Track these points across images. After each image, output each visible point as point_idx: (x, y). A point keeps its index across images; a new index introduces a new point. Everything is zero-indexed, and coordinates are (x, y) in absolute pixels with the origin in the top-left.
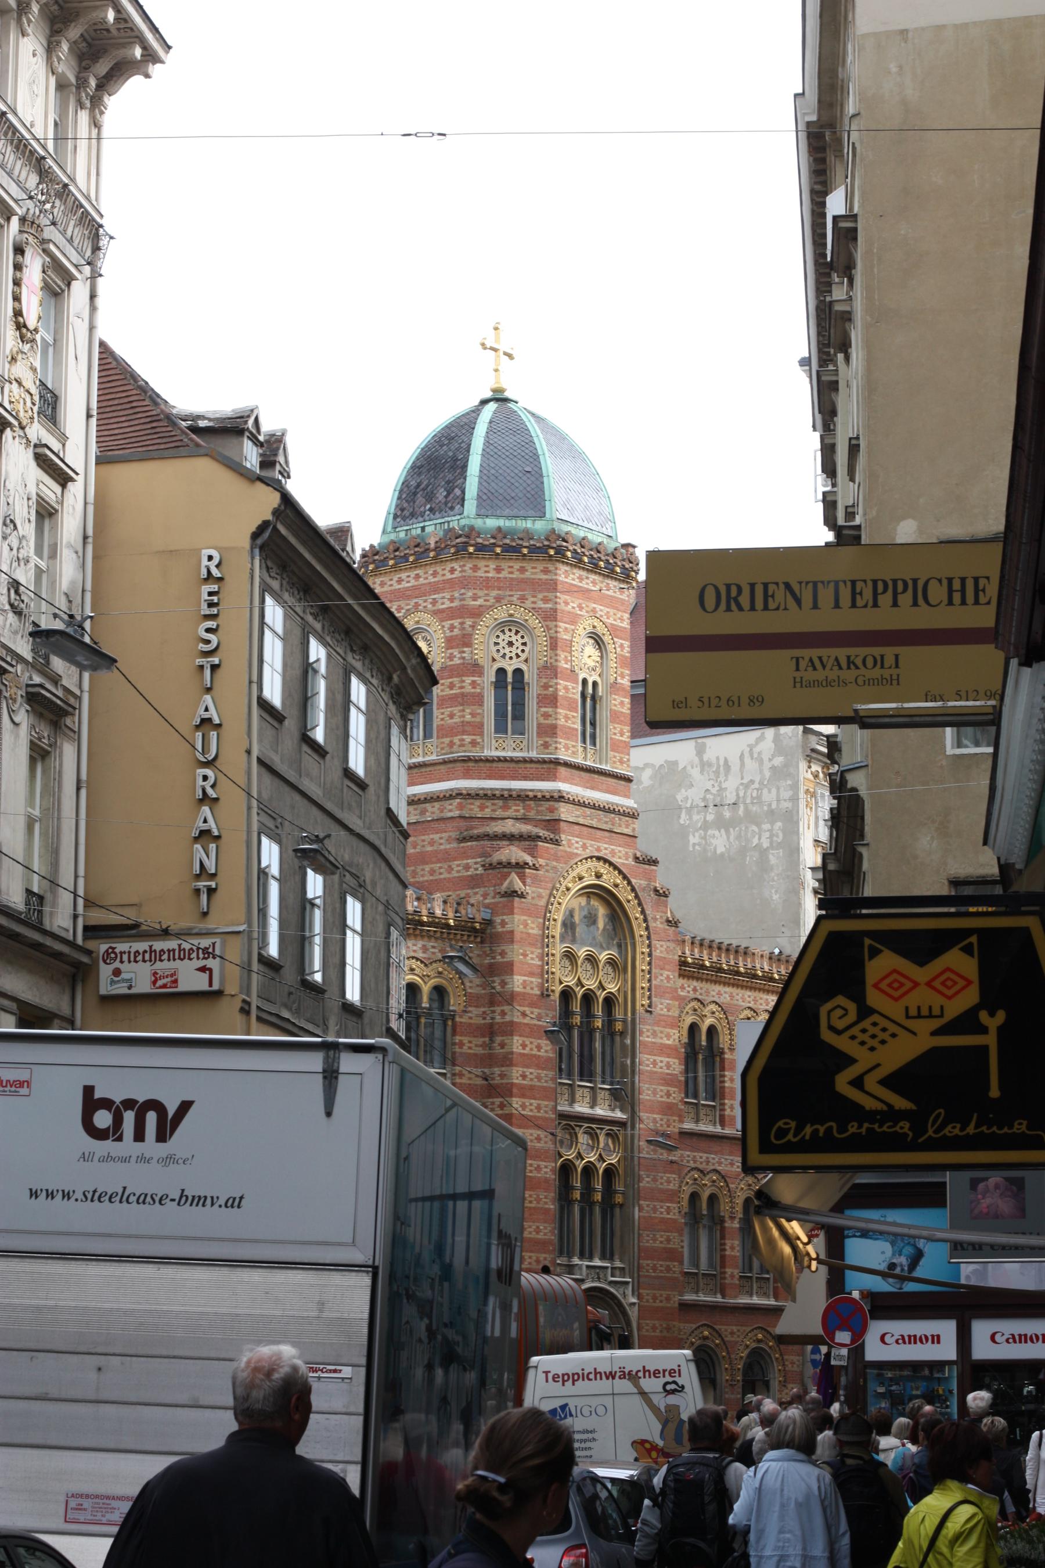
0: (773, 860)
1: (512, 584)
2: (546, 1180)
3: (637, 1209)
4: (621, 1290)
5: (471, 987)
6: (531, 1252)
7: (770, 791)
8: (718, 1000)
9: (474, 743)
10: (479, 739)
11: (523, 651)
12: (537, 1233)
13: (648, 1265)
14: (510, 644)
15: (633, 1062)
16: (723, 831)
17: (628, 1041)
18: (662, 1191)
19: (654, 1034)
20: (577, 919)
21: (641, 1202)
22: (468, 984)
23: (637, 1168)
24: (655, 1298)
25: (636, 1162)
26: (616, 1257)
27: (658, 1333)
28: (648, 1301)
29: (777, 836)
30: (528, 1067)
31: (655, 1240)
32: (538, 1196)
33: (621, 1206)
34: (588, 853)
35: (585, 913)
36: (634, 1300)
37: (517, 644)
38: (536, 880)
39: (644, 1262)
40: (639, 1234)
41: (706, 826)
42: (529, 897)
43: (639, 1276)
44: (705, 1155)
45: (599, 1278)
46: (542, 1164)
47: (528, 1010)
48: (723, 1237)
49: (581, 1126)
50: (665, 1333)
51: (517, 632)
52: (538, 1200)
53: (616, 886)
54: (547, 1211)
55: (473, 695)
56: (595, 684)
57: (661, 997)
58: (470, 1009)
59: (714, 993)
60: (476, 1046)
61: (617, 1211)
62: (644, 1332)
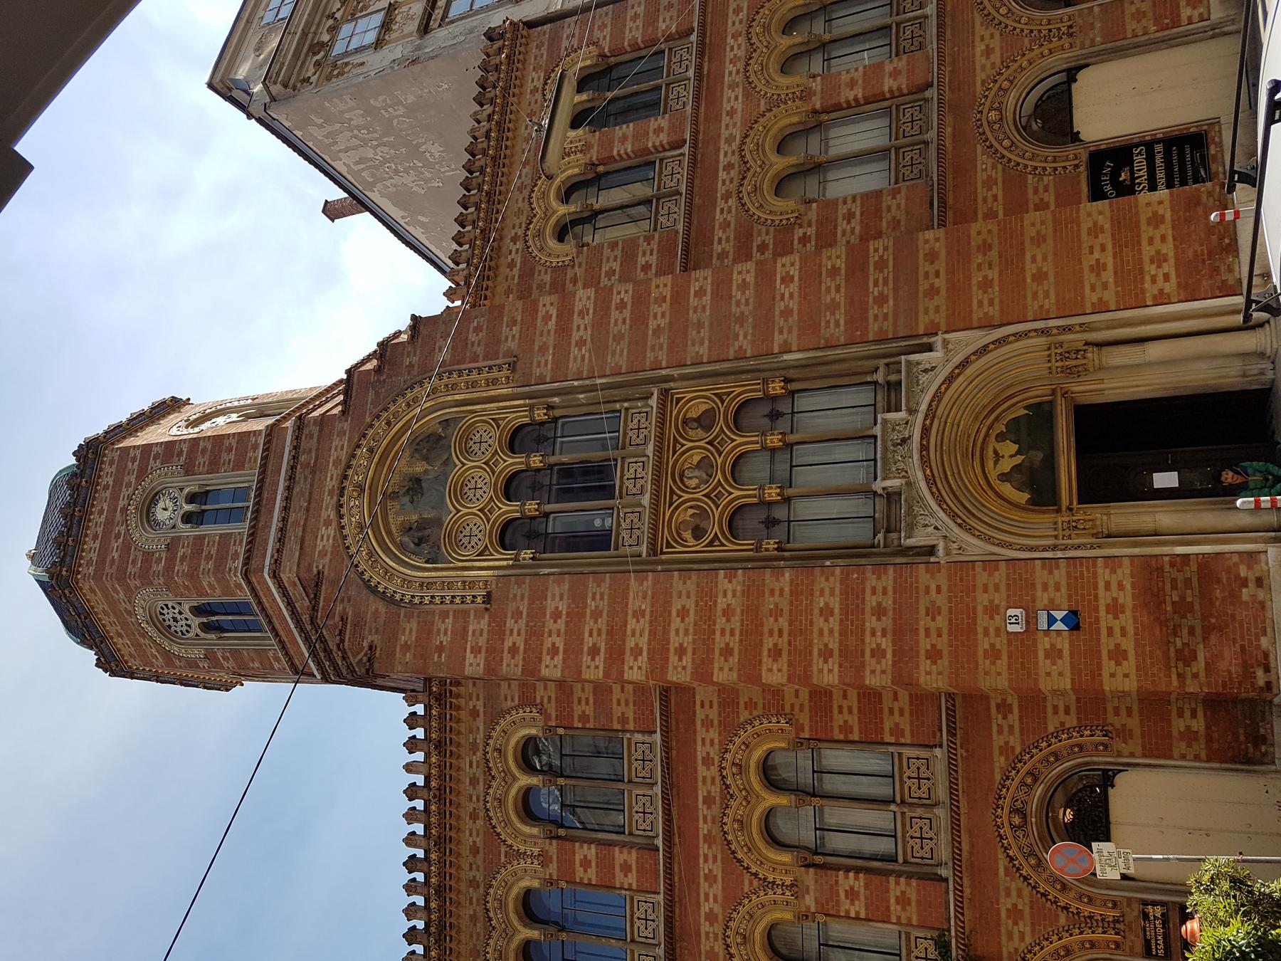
0: (411, 99)
1: (124, 624)
2: (746, 593)
3: (786, 357)
4: (924, 378)
5: (513, 700)
6: (863, 631)
7: (351, 119)
8: (529, 189)
9: (277, 659)
10: (271, 654)
11: (173, 608)
13: (876, 316)
14: (175, 620)
16: (423, 149)
17: (556, 399)
19: (543, 349)
20: (415, 517)
22: (509, 704)
23: (726, 365)
24: (933, 292)
25: (717, 367)
26: (869, 379)
27: (993, 274)
28: (937, 310)
29: (385, 100)
31: (834, 306)
33: (787, 380)
34: (333, 515)
35: (406, 499)
36: (938, 340)
37: (171, 615)
38: (359, 626)
39: (873, 327)
41: (428, 165)
42: (376, 638)
43: (895, 339)
44: (722, 175)
45: (904, 441)
46: (721, 603)
47: (508, 643)
48: (838, 107)
50: (994, 254)
51: (161, 614)
52: (777, 612)
53: (371, 450)
54: (795, 593)
55: (236, 660)
56: (191, 499)
57: (499, 341)
58: (538, 701)
59: (520, 204)
60: (583, 690)
62: (994, 311)
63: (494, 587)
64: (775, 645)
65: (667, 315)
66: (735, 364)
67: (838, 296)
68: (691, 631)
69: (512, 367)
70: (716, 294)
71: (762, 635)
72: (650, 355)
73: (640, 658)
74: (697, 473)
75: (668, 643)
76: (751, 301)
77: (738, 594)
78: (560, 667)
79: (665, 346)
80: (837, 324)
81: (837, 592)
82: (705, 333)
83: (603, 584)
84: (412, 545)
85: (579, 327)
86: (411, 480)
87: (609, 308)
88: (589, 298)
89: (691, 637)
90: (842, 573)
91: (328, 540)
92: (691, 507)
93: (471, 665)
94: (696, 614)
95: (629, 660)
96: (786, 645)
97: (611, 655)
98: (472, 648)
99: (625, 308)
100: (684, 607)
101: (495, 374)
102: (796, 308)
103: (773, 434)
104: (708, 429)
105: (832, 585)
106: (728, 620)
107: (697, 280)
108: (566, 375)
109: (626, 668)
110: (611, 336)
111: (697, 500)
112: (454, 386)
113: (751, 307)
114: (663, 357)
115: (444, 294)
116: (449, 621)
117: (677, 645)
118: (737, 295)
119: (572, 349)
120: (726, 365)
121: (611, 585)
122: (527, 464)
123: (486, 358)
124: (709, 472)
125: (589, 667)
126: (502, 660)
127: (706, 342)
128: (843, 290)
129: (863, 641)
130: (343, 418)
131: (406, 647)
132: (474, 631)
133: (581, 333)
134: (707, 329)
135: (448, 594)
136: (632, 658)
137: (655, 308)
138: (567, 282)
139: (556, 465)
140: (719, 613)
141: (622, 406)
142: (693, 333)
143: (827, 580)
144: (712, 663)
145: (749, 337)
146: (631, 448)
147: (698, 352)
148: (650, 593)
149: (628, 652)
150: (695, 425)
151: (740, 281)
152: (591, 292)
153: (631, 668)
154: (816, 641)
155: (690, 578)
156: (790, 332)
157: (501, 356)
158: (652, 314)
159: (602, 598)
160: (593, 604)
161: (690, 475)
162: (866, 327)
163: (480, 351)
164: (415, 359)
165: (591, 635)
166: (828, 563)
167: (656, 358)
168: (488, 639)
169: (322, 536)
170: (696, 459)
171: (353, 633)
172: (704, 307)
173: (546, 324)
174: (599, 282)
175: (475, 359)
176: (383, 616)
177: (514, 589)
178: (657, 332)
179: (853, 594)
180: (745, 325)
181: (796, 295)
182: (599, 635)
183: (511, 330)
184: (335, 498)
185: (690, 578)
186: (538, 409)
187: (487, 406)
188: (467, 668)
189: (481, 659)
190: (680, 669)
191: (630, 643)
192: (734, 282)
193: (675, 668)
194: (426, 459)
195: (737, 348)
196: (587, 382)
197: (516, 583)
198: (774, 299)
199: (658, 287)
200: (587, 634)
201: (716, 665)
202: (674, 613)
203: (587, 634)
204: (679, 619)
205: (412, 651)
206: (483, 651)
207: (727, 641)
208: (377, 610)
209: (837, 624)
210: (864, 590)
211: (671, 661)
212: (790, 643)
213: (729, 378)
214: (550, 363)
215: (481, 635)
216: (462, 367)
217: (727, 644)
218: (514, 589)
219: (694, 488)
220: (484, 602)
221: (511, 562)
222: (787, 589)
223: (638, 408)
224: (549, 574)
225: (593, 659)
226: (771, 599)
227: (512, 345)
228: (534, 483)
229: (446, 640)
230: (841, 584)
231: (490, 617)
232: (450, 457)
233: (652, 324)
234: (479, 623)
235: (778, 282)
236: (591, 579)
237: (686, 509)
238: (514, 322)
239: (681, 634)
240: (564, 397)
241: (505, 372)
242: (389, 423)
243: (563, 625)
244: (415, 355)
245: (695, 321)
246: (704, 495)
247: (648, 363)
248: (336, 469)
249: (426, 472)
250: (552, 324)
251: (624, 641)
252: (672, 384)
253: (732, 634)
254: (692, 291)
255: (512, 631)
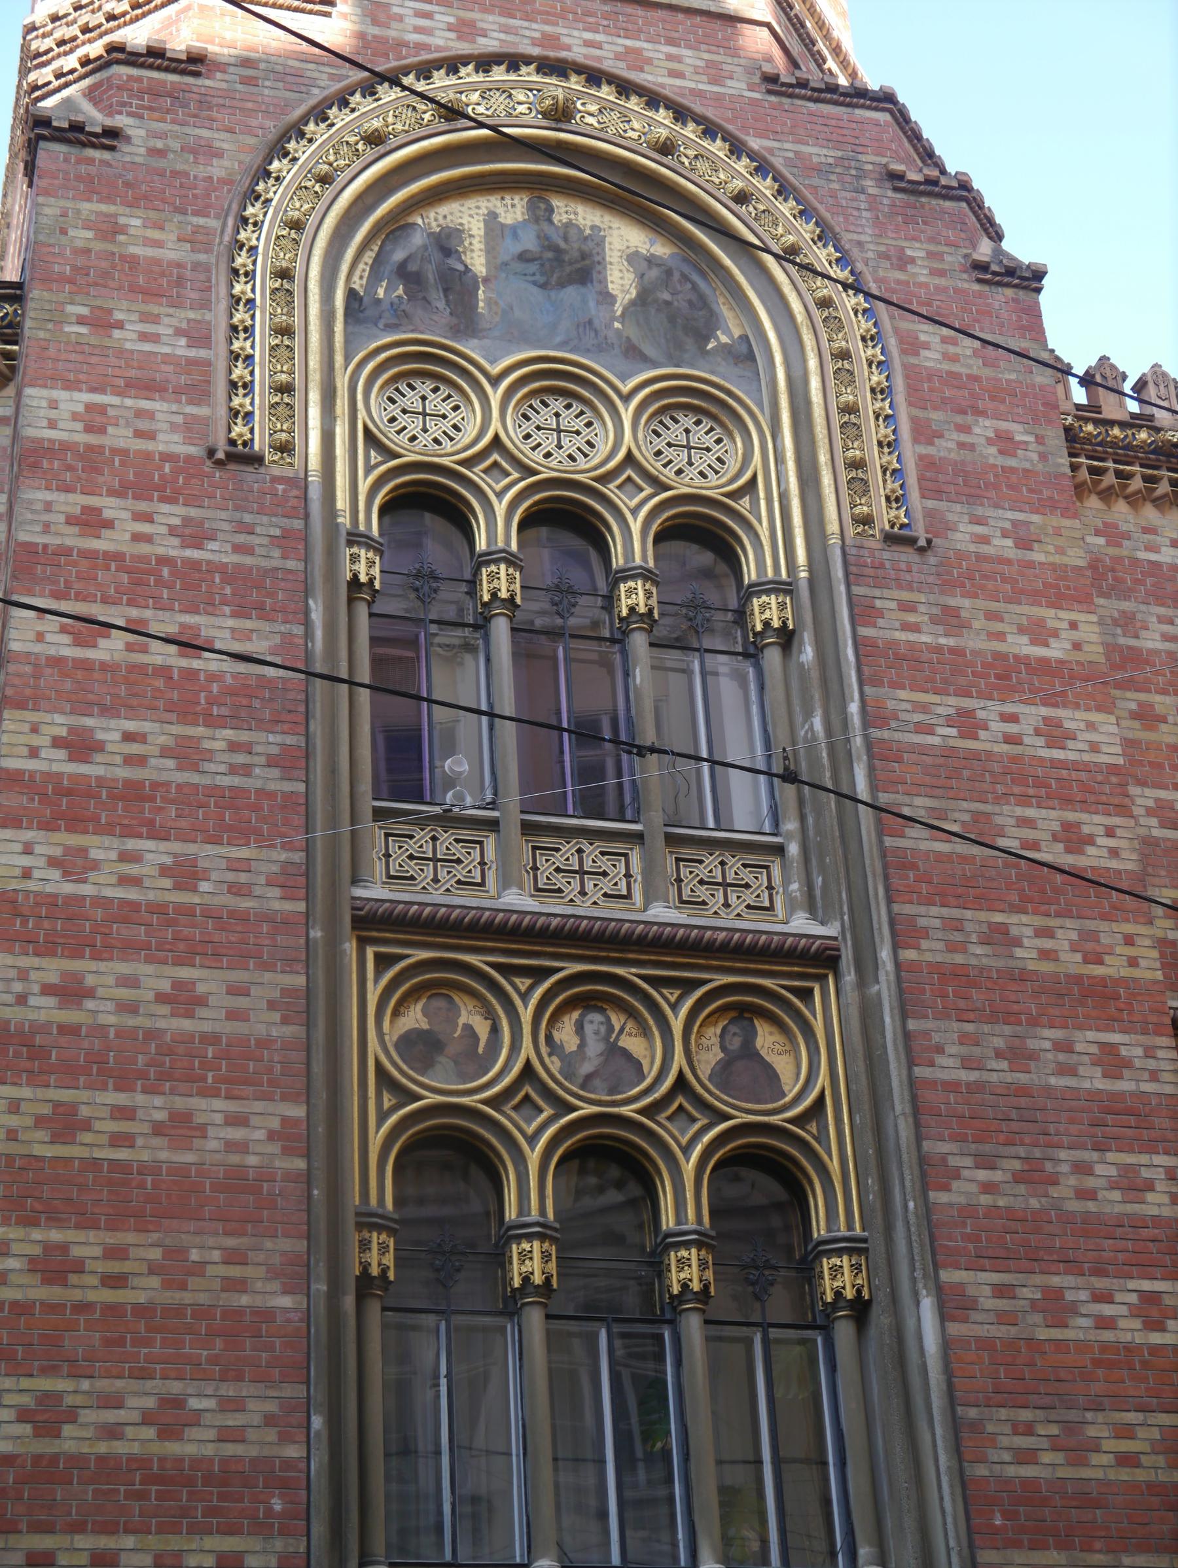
3: (927, 1304)
6: (109, 1529)
12: (169, 1432)
15: (837, 725)
18: (1092, 1226)
19: (950, 619)
20: (477, 261)
21: (946, 1276)
25: (900, 1103)
30: (106, 711)
32: (175, 1254)
33: (860, 1309)
34: (488, 44)
35: (529, 242)
40: (956, 1426)
42: (136, 149)
47: (111, 507)
49: (540, 974)
53: (666, 148)
57: (973, 498)
61: (844, 1331)
63: (276, 471)
64: (79, 1267)
65: (1046, 967)
66: (908, 1156)
67: (1106, 1459)
68: (131, 1021)
69: (896, 539)
70: (1111, 1105)
71: (112, 1227)
72: (931, 916)
73: (56, 874)
74: (595, 1048)
75: (96, 957)
76: (1091, 1206)
77: (234, 1159)
78: (38, 648)
79: (959, 959)
80: (1026, 1457)
81: (230, 1449)
82: (999, 1073)
83: (275, 772)
84: (399, 256)
85: (1013, 718)
86: (584, 256)
87: (1067, 802)
88: (1095, 748)
89: (112, 1019)
90: (288, 1464)
91: (418, 30)
92: (495, 1030)
93: (53, 405)
94: (186, 1039)
95: (51, 843)
96: (77, 1295)
97: (69, 792)
98: (102, 409)
99: (1069, 850)
100: (202, 1001)
101: (880, 487)
102: (1069, 1334)
103: (703, 1265)
104: (723, 1074)
105: (251, 1435)
106: (158, 1129)
107: (1149, 1053)
108: (876, 682)
109: (29, 835)
110: (988, 808)
111: (515, 1047)
112: (846, 377)
113: (1074, 1206)
114: (930, 951)
115: (1104, 359)
116: (181, 348)
117: (90, 980)
118: (1108, 1165)
119: (952, 701)
120: (905, 1131)
121: (271, 795)
122: (626, 574)
123: (927, 464)
124: (597, 1082)
125: (35, 730)
126: (67, 489)
127: (973, 1076)
128: (1125, 1474)
129: (78, 1528)
130: (757, 79)
131: (111, 230)
132: (150, 415)
133: (997, 726)
134: (1009, 1077)
135: (260, 345)
136: (58, 852)
137: (1067, 933)
138: (1143, 696)
139: (624, 653)
140: (180, 1103)
141: (789, 836)
142: (998, 1036)
143: (269, 1420)
144: (34, 1078)
145: (985, 1199)
146: (670, 861)
147: (940, 1050)
148: (246, 904)
149: (76, 840)
150: (735, 1043)
151: (1145, 1173)
152: (1112, 755)
153: (28, 850)
154: (85, 1385)
155: (285, 1021)
156: (1004, 1318)
157: (930, 504)
158: (1052, 922)
159: (233, 770)
160: (220, 745)
161: (589, 1029)
162: (1017, 1544)
163: (946, 447)
164: (921, 273)
165: (128, 737)
166: (317, 1422)
167: (925, 933)
168: (124, 453)
169: (428, 15)
170: (633, 1044)
171: (155, 92)
172: (1070, 1071)
173: (1021, 630)
174: (1143, 783)
175: (924, 433)
176: (201, 171)
177: (268, 527)
178: (999, 937)
179: (222, 1497)
180: (1022, 1189)
181: (1108, 1336)
182: (129, 760)
183: (1005, 535)
184: (536, 51)
185: (285, 1021)
186: (782, 606)
187: (791, 465)
188: (44, 393)
189: (72, 433)
190: (18, 987)
191: (102, 848)
192: (1144, 1159)
193: (23, 975)
194: (644, 299)
195: (953, 1161)
196: (858, 742)
197: (287, 534)
198: (1099, 1272)
199: (1129, 940)
200: (131, 726)
201: (26, 1092)
202: (184, 973)
203: (131, 726)
204: (165, 986)
205: (98, 246)
206: (93, 439)
207: (98, 1126)
208: (219, 154)
209: (136, 1449)
210: (230, 1531)
211: (45, 962)
212: (83, 1307)
213: (869, 1137)
214: (912, 637)
215: (139, 434)
216: (900, 397)
217: (86, 1126)
218: (268, 527)
219: (549, 1039)
220: (233, 442)
221: (344, 520)
222: (245, 1300)
223: (786, 882)
224: (307, 623)
225: (57, 742)
226: (216, 1255)
227: (963, 536)
228: (570, 591)
229: (127, 338)
230: (254, 1461)
231: (189, 459)
232: (648, 362)
233: (1022, 924)
234: (174, 428)
235: (1146, 1285)
236: (290, 740)
237: (490, 1015)
238: (1025, 544)
239: (124, 993)
240: (815, 675)
241: (884, 516)
242: (742, 198)
243: (159, 660)
244: (934, 272)
245: (1032, 1044)
246: (528, 1064)
247: (908, 909)
248: (618, 57)
249: (609, 298)
250: (1020, 645)
251: (108, 830)
252: (849, 978)
253: (119, 1141)
254: (1115, 1038)
255: (148, 518)
